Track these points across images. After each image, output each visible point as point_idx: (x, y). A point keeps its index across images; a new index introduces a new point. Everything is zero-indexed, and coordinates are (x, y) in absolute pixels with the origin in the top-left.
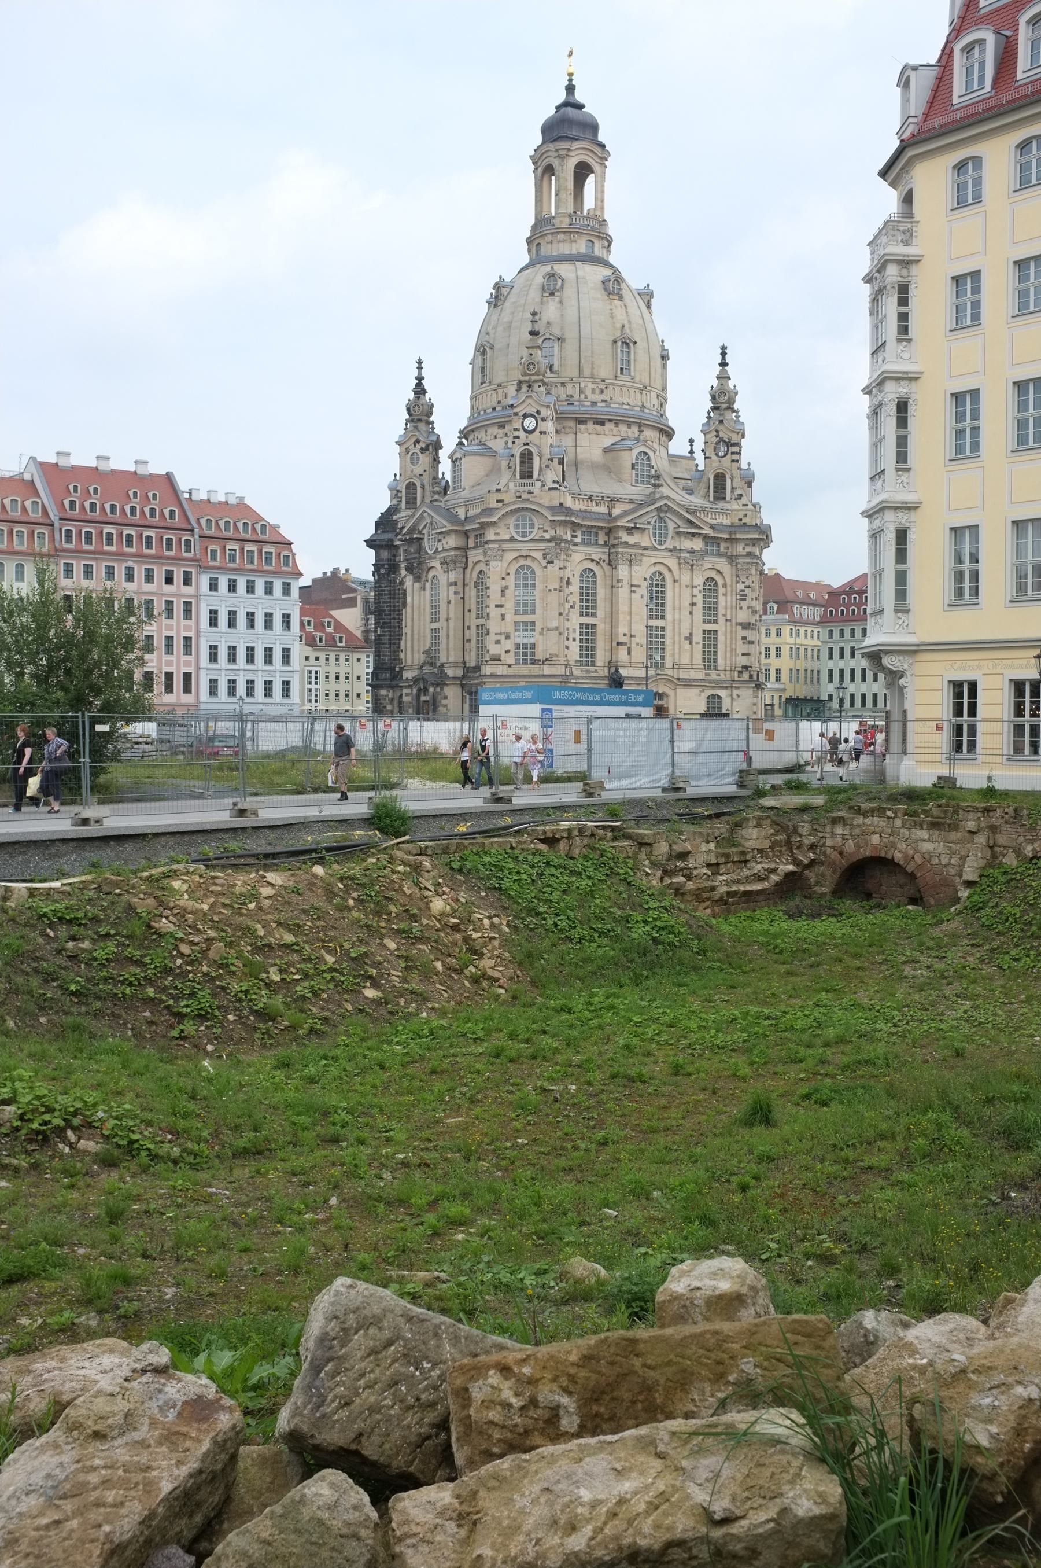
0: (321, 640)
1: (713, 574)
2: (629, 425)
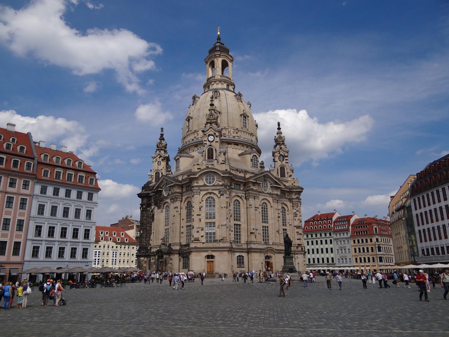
0: (119, 240)
1: (284, 206)
2: (247, 146)
